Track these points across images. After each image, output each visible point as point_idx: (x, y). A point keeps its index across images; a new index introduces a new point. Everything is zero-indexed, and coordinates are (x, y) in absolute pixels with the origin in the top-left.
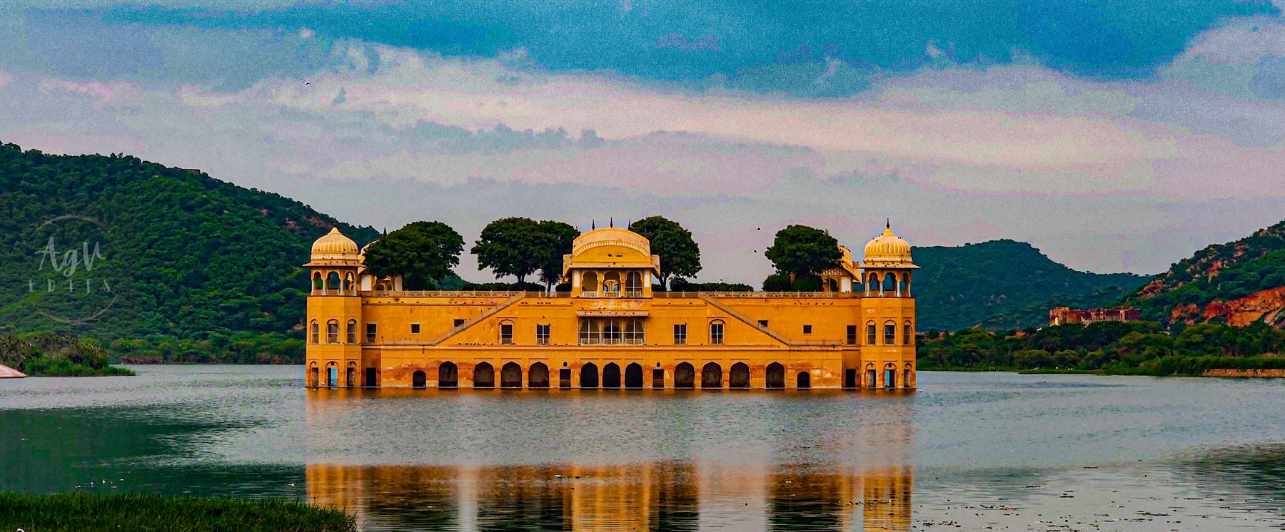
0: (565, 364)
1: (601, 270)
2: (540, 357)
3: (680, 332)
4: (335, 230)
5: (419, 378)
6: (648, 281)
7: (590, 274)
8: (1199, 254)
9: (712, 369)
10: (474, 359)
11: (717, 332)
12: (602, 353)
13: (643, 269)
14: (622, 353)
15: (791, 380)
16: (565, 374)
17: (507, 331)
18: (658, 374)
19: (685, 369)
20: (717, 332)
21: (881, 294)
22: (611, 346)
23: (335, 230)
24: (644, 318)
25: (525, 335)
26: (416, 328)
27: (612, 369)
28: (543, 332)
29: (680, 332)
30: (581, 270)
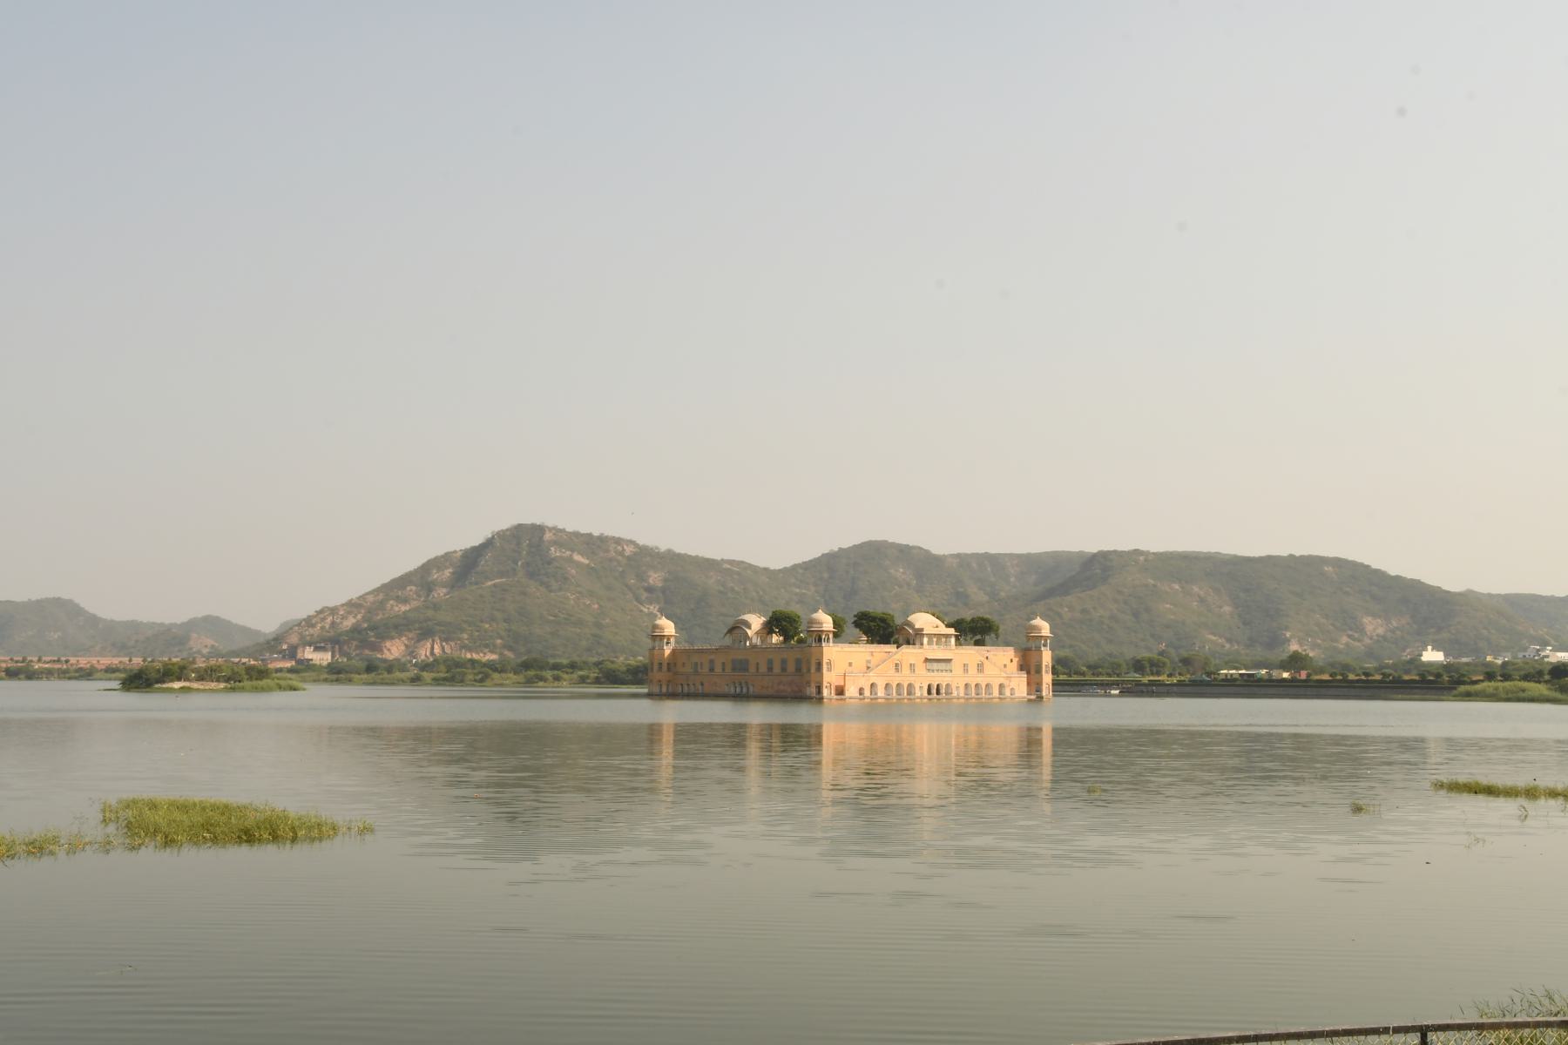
2: (911, 680)
5: (861, 691)
7: (930, 635)
8: (321, 612)
11: (980, 667)
15: (1007, 693)
20: (980, 667)
24: (949, 661)
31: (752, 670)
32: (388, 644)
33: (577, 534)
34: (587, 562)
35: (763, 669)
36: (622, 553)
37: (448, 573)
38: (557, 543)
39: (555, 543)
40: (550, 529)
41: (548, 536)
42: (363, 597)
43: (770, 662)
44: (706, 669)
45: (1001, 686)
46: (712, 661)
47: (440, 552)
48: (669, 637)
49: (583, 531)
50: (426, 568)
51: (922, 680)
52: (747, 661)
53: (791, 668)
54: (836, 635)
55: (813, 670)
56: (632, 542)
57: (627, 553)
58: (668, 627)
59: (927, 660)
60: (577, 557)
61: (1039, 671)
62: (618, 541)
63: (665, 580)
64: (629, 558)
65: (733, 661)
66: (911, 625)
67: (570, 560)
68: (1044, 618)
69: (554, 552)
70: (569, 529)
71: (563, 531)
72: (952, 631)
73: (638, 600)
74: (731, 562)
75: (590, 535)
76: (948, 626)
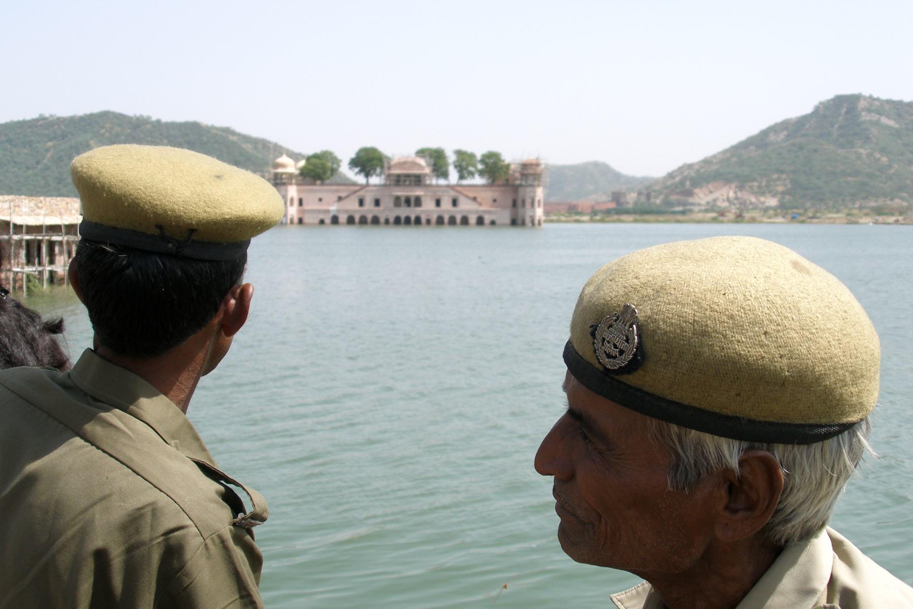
3: (438, 203)
5: (322, 222)
11: (455, 203)
12: (403, 212)
14: (413, 212)
20: (455, 203)
26: (320, 200)
28: (377, 203)
29: (438, 203)
32: (697, 191)
33: (889, 102)
34: (891, 123)
37: (782, 135)
38: (869, 110)
39: (863, 110)
40: (865, 98)
41: (862, 104)
42: (714, 156)
47: (779, 119)
49: (896, 98)
50: (765, 133)
60: (884, 120)
67: (877, 123)
69: (865, 117)
70: (884, 96)
71: (878, 99)
75: (900, 103)
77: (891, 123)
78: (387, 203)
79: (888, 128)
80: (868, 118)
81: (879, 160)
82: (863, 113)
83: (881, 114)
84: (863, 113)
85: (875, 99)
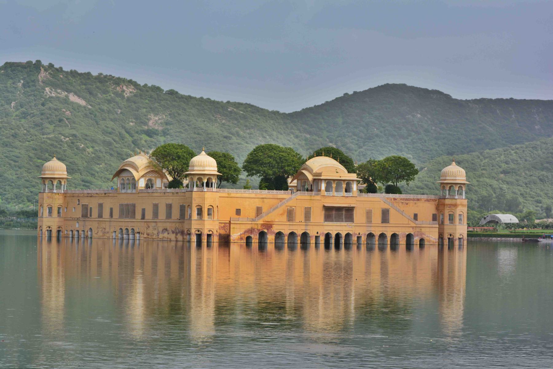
0: (317, 233)
1: (334, 180)
4: (203, 153)
6: (355, 187)
7: (329, 182)
9: (382, 236)
10: (276, 229)
11: (385, 216)
13: (353, 180)
16: (317, 238)
17: (290, 215)
18: (359, 238)
19: (370, 236)
20: (385, 216)
21: (456, 197)
22: (338, 223)
23: (203, 153)
25: (300, 216)
26: (238, 212)
27: (338, 236)
29: (369, 214)
30: (325, 180)
31: (138, 215)
33: (74, 73)
34: (82, 103)
35: (149, 215)
36: (120, 95)
38: (54, 86)
43: (156, 207)
44: (95, 213)
45: (409, 237)
46: (101, 206)
48: (60, 180)
51: (320, 227)
52: (134, 206)
53: (176, 213)
54: (220, 178)
55: (195, 216)
56: (131, 82)
57: (127, 94)
58: (56, 168)
59: (324, 206)
60: (73, 98)
61: (452, 218)
62: (118, 81)
63: (167, 124)
64: (128, 100)
65: (121, 205)
66: (310, 171)
67: (66, 101)
68: (459, 163)
71: (60, 70)
72: (353, 176)
73: (134, 142)
74: (238, 105)
76: (350, 170)
77: (82, 103)
78: (318, 215)
79: (79, 106)
80: (53, 95)
81: (84, 150)
82: (47, 89)
83: (69, 91)
84: (47, 89)
85: (57, 69)
